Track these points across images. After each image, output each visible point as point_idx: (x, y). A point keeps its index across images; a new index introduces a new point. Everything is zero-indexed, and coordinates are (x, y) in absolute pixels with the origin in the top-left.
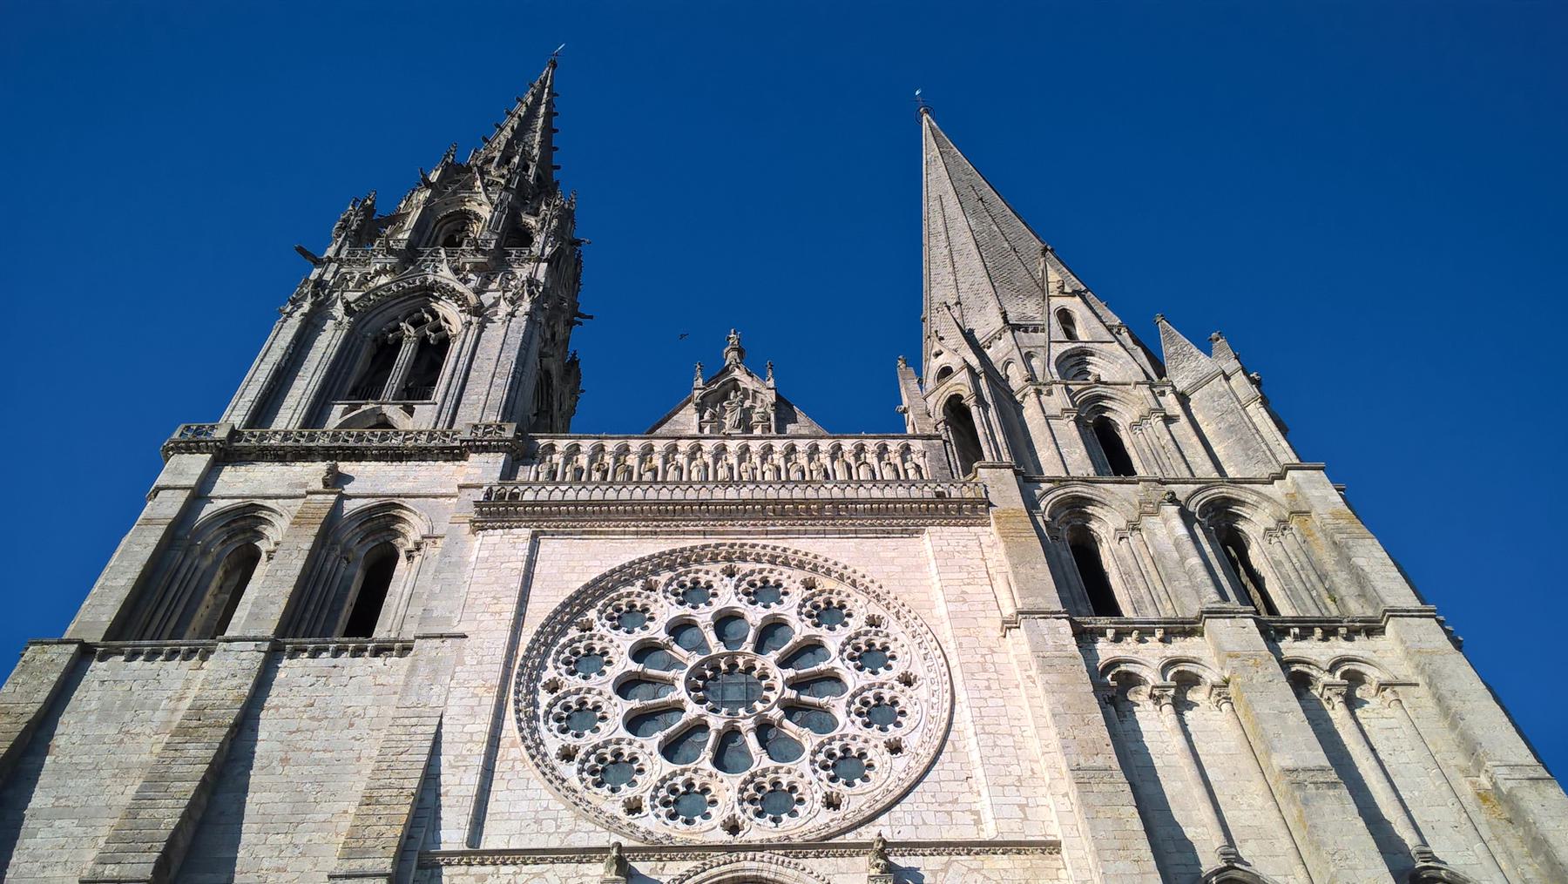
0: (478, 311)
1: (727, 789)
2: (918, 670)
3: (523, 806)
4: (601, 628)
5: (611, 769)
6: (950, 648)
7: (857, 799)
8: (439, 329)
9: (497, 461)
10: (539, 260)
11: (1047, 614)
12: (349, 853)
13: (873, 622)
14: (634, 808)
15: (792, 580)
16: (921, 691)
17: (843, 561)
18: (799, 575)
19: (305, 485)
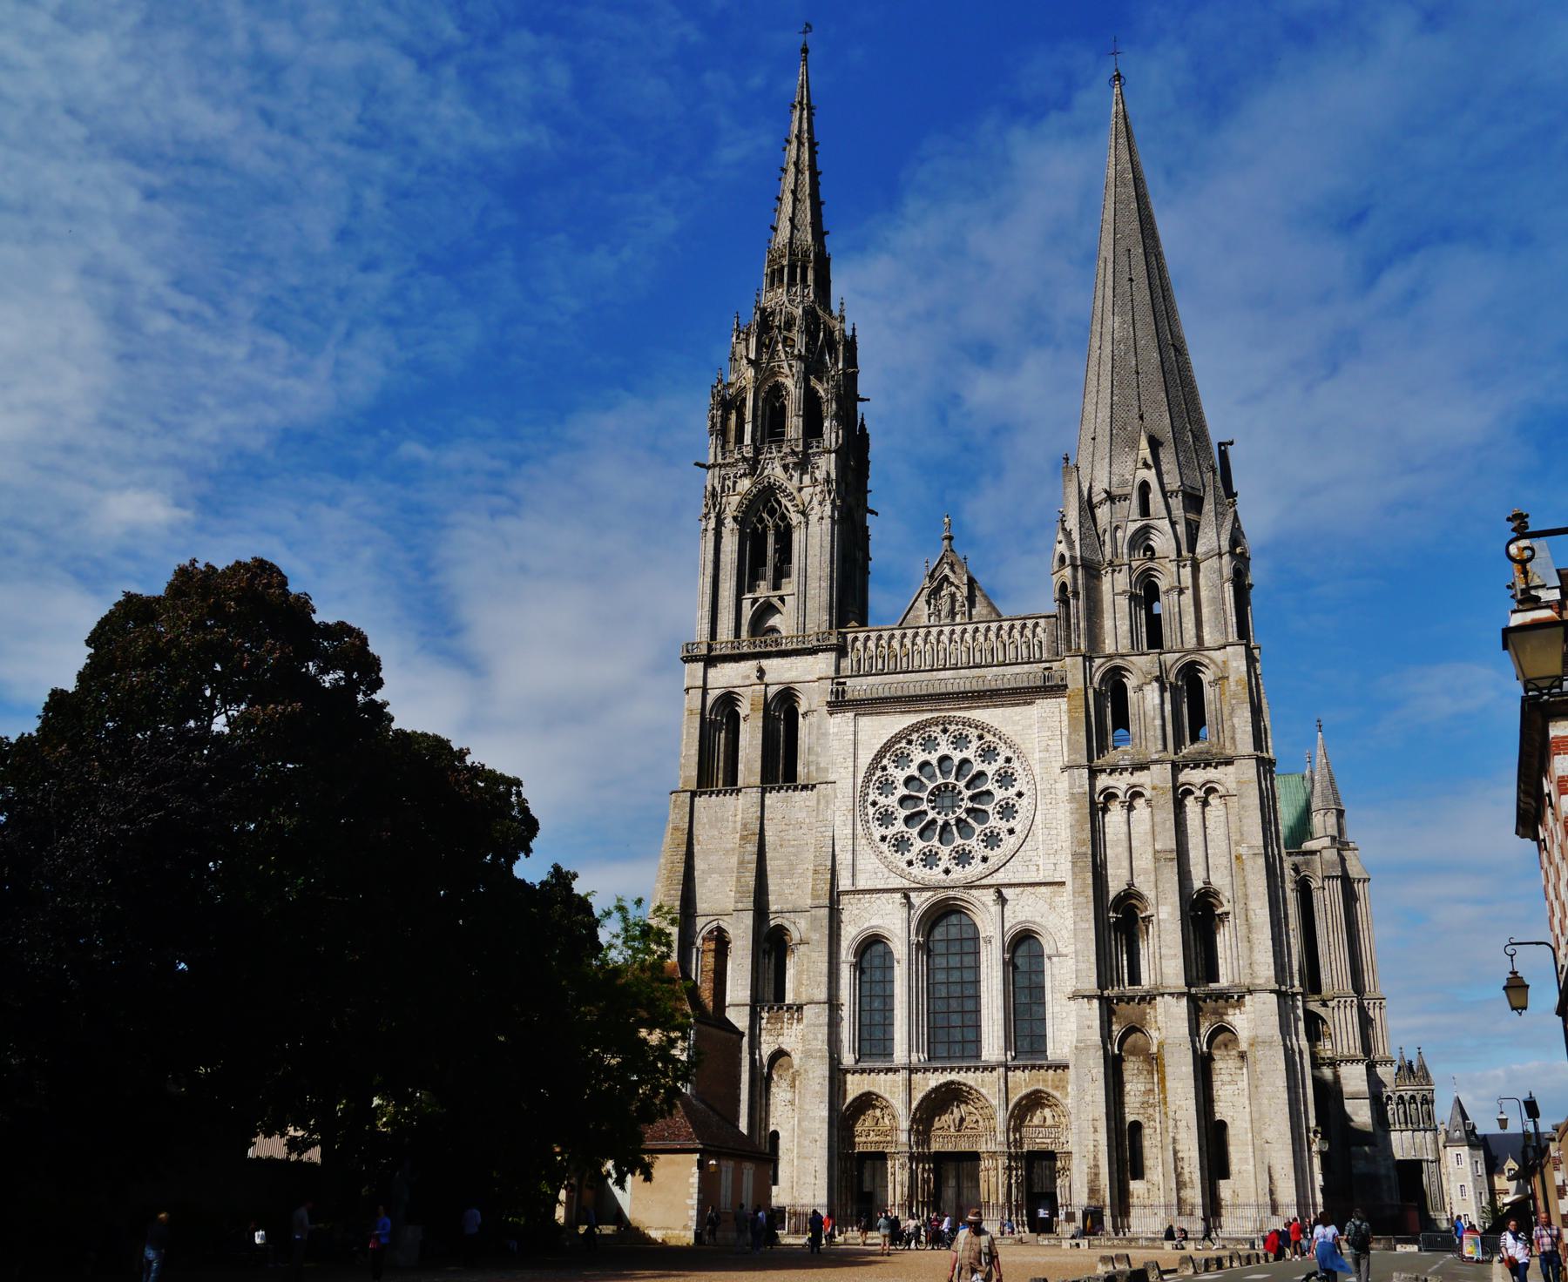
0: (803, 513)
1: (945, 852)
2: (1024, 790)
3: (869, 867)
4: (891, 770)
5: (901, 844)
6: (1038, 778)
7: (996, 855)
8: (783, 517)
9: (833, 655)
10: (830, 452)
11: (1079, 767)
12: (815, 897)
13: (1008, 760)
14: (910, 863)
15: (973, 734)
16: (1024, 801)
17: (996, 725)
18: (976, 733)
19: (748, 677)
